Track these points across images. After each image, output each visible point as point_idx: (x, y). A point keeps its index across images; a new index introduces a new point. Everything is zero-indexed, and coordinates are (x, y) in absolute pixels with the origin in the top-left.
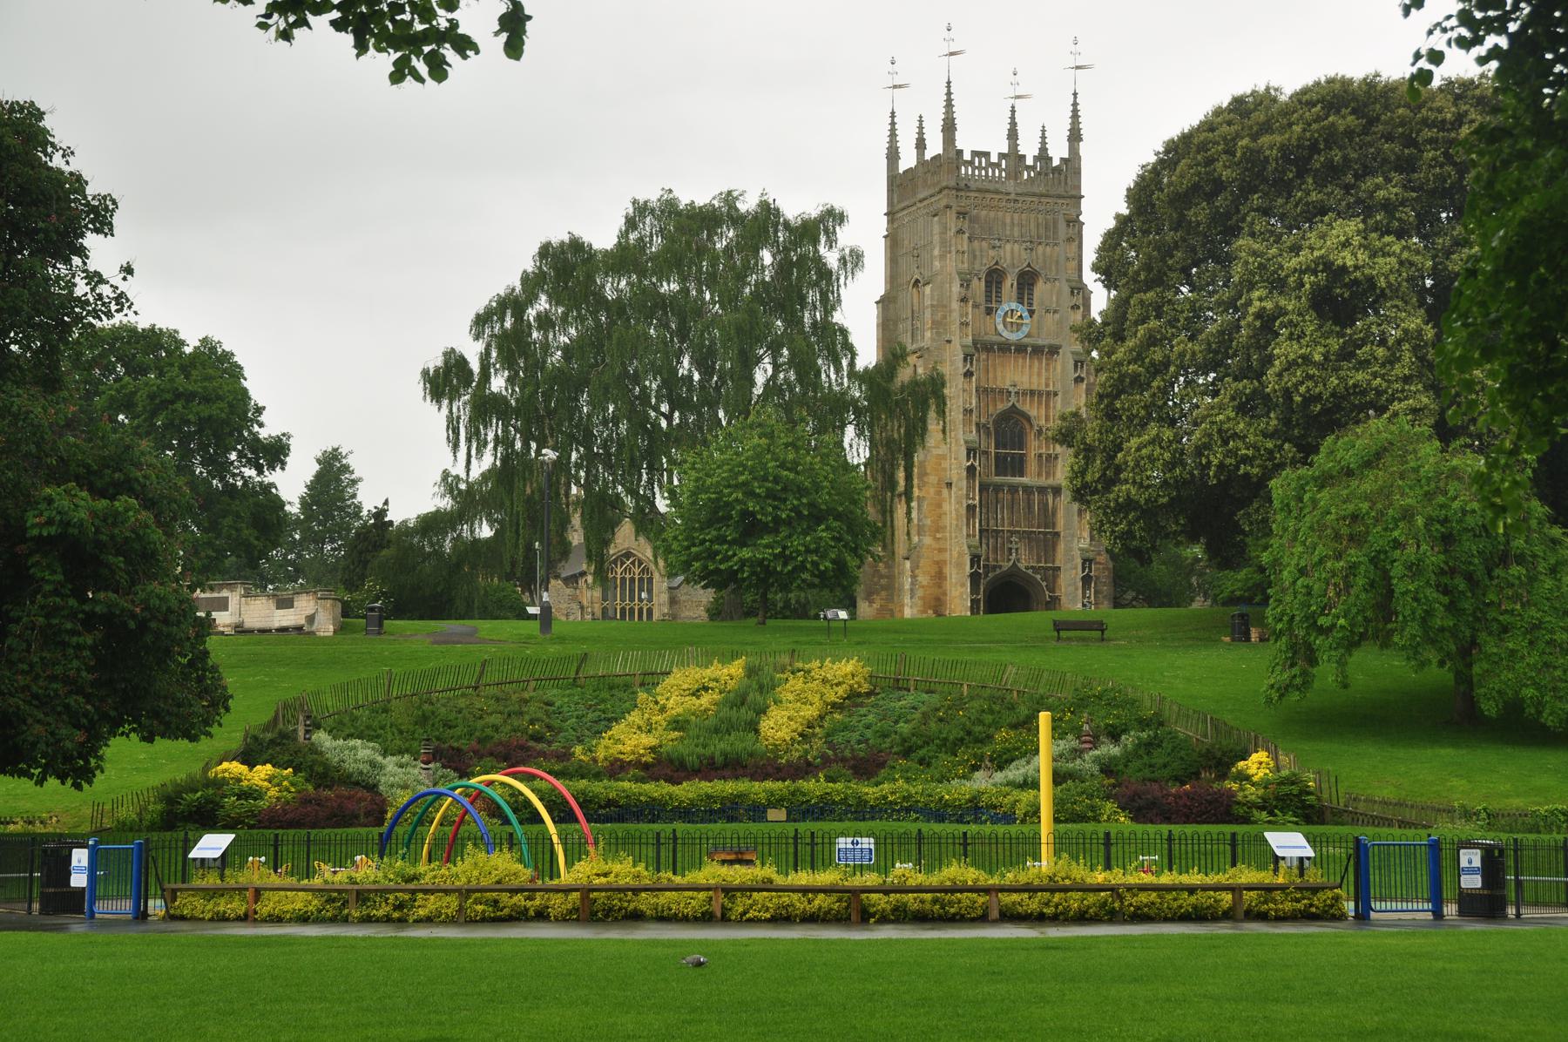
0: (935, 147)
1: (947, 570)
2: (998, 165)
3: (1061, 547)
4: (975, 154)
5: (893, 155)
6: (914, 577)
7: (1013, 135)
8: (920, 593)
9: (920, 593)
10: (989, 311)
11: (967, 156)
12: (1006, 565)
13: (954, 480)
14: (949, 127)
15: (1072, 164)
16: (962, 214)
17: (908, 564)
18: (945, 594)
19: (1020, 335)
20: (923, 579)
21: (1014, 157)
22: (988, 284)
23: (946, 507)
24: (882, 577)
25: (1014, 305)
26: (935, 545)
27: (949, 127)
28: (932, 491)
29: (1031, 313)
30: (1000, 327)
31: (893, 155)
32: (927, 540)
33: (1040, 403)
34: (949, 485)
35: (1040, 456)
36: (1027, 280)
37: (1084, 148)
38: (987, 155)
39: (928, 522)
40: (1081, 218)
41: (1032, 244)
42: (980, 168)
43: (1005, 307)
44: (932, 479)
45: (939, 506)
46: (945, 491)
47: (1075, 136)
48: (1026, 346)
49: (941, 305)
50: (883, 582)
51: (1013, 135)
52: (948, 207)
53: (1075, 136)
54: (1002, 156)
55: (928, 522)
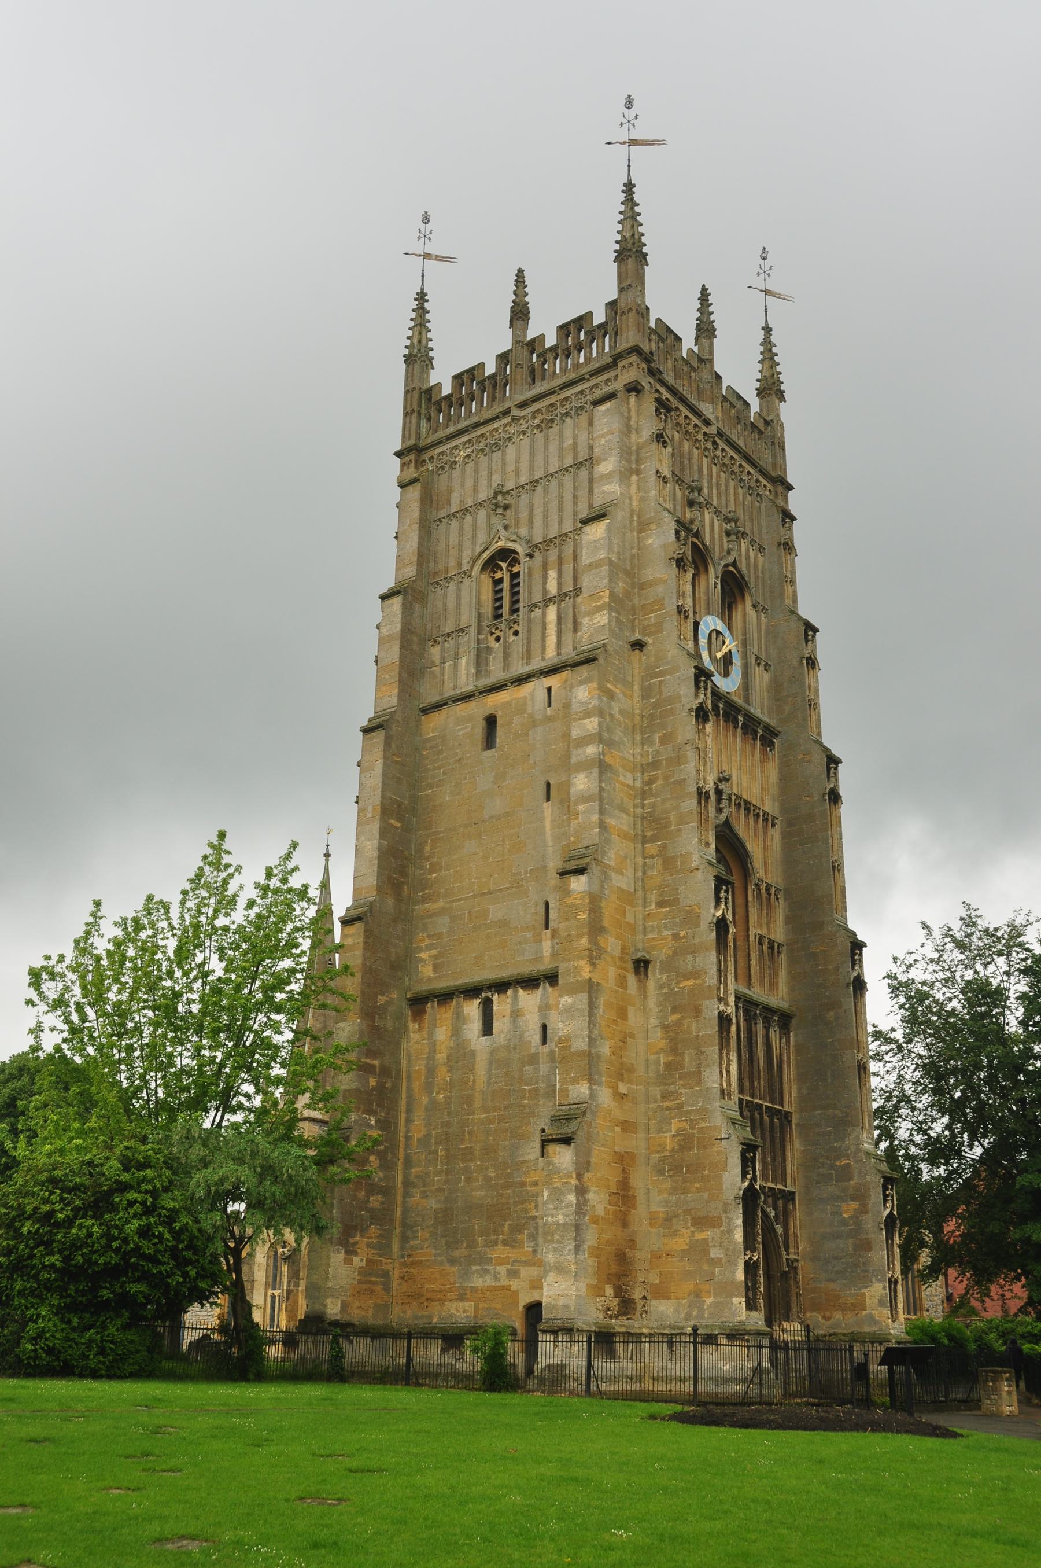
0: (594, 291)
1: (641, 1180)
3: (795, 1147)
5: (418, 357)
6: (581, 1191)
8: (591, 1238)
9: (591, 1238)
13: (659, 955)
14: (631, 254)
15: (768, 431)
16: (662, 406)
17: (564, 1157)
18: (632, 1243)
20: (598, 1200)
23: (634, 1018)
24: (373, 1189)
25: (720, 626)
26: (617, 1114)
27: (631, 254)
28: (612, 972)
31: (418, 357)
32: (605, 1097)
33: (756, 829)
34: (641, 966)
35: (761, 938)
37: (786, 411)
39: (605, 1049)
44: (611, 944)
45: (622, 1013)
46: (632, 979)
48: (738, 710)
49: (627, 569)
50: (375, 1201)
52: (634, 388)
55: (605, 1049)
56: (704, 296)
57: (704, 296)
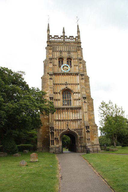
2: (60, 38)
4: (55, 36)
7: (64, 32)
10: (60, 67)
11: (53, 36)
12: (67, 129)
15: (78, 37)
19: (68, 71)
21: (64, 36)
22: (59, 61)
29: (71, 67)
30: (62, 69)
36: (69, 60)
38: (57, 36)
40: (82, 47)
41: (69, 52)
42: (56, 39)
43: (63, 65)
47: (78, 32)
51: (64, 32)
53: (78, 32)
54: (62, 36)
56: (64, 28)
57: (64, 28)
